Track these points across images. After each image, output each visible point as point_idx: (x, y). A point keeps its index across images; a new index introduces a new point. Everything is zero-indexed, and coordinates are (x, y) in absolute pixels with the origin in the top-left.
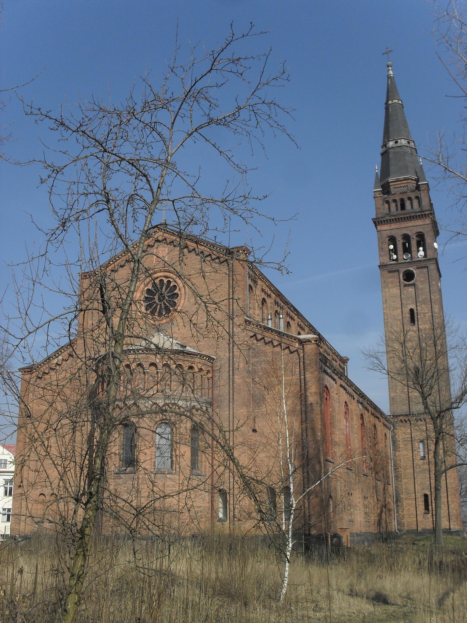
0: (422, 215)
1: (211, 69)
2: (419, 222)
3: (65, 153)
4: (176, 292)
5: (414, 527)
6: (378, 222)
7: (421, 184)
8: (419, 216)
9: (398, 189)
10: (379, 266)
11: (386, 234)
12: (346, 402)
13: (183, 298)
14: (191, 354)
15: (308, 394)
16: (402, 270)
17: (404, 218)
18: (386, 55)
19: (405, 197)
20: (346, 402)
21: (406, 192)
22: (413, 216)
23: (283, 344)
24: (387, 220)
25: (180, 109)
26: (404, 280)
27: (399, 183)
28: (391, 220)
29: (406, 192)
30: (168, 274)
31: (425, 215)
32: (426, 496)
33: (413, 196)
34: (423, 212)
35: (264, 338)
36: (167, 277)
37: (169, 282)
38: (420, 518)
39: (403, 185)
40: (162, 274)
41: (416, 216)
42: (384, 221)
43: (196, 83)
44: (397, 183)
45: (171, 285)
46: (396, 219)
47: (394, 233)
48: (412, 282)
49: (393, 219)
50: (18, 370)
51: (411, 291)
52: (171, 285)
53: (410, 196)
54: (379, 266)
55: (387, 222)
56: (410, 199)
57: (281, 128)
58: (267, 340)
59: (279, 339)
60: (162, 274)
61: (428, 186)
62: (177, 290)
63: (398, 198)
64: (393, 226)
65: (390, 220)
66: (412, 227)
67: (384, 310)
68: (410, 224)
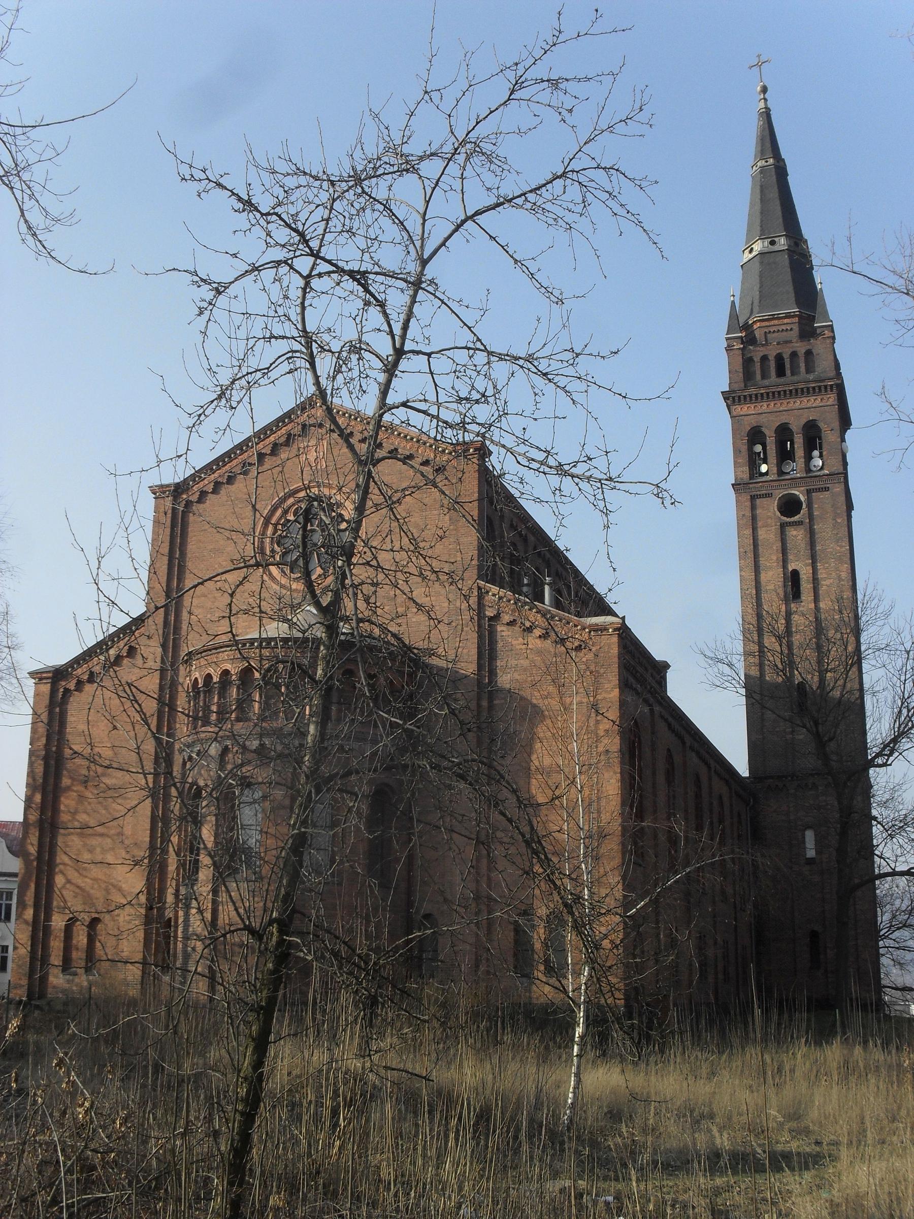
0: (820, 387)
1: (509, 99)
2: (814, 401)
3: (235, 255)
6: (733, 398)
7: (819, 327)
8: (814, 388)
9: (776, 334)
10: (733, 485)
11: (748, 424)
12: (669, 750)
16: (779, 494)
17: (785, 391)
18: (756, 69)
20: (669, 750)
21: (790, 342)
22: (802, 389)
24: (750, 396)
25: (443, 173)
26: (782, 513)
27: (776, 322)
28: (759, 396)
29: (790, 342)
31: (826, 387)
32: (814, 935)
34: (823, 381)
39: (784, 327)
41: (808, 388)
42: (745, 396)
43: (477, 123)
44: (772, 323)
46: (768, 394)
47: (763, 420)
48: (796, 518)
49: (762, 394)
50: (28, 676)
51: (796, 536)
53: (798, 349)
54: (733, 485)
55: (751, 400)
57: (632, 218)
61: (833, 331)
63: (772, 352)
64: (764, 407)
65: (756, 395)
66: (797, 411)
67: (741, 570)
68: (797, 403)
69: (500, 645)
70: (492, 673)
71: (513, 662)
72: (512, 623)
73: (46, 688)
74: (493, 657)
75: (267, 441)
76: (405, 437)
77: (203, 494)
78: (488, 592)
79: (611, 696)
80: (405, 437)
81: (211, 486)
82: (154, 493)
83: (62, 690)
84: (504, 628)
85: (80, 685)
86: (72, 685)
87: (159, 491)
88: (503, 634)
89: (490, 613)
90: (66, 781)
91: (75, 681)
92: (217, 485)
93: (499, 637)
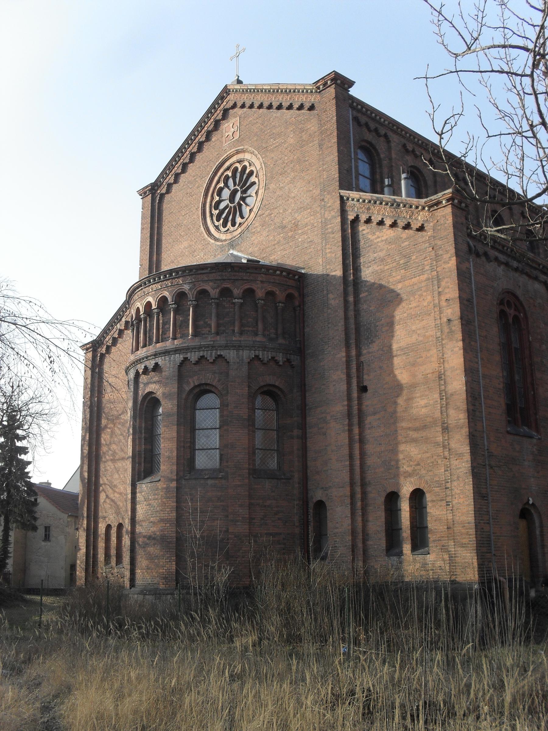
15: (443, 303)
30: (240, 156)
37: (244, 168)
69: (362, 243)
70: (357, 270)
71: (372, 256)
72: (368, 221)
73: (90, 355)
74: (356, 255)
75: (203, 132)
76: (286, 91)
77: (170, 186)
78: (348, 199)
79: (449, 265)
80: (286, 91)
81: (173, 178)
82: (141, 195)
83: (99, 355)
84: (364, 227)
85: (108, 349)
86: (104, 350)
87: (143, 193)
88: (364, 232)
89: (351, 217)
90: (104, 422)
91: (105, 347)
92: (177, 176)
93: (361, 236)
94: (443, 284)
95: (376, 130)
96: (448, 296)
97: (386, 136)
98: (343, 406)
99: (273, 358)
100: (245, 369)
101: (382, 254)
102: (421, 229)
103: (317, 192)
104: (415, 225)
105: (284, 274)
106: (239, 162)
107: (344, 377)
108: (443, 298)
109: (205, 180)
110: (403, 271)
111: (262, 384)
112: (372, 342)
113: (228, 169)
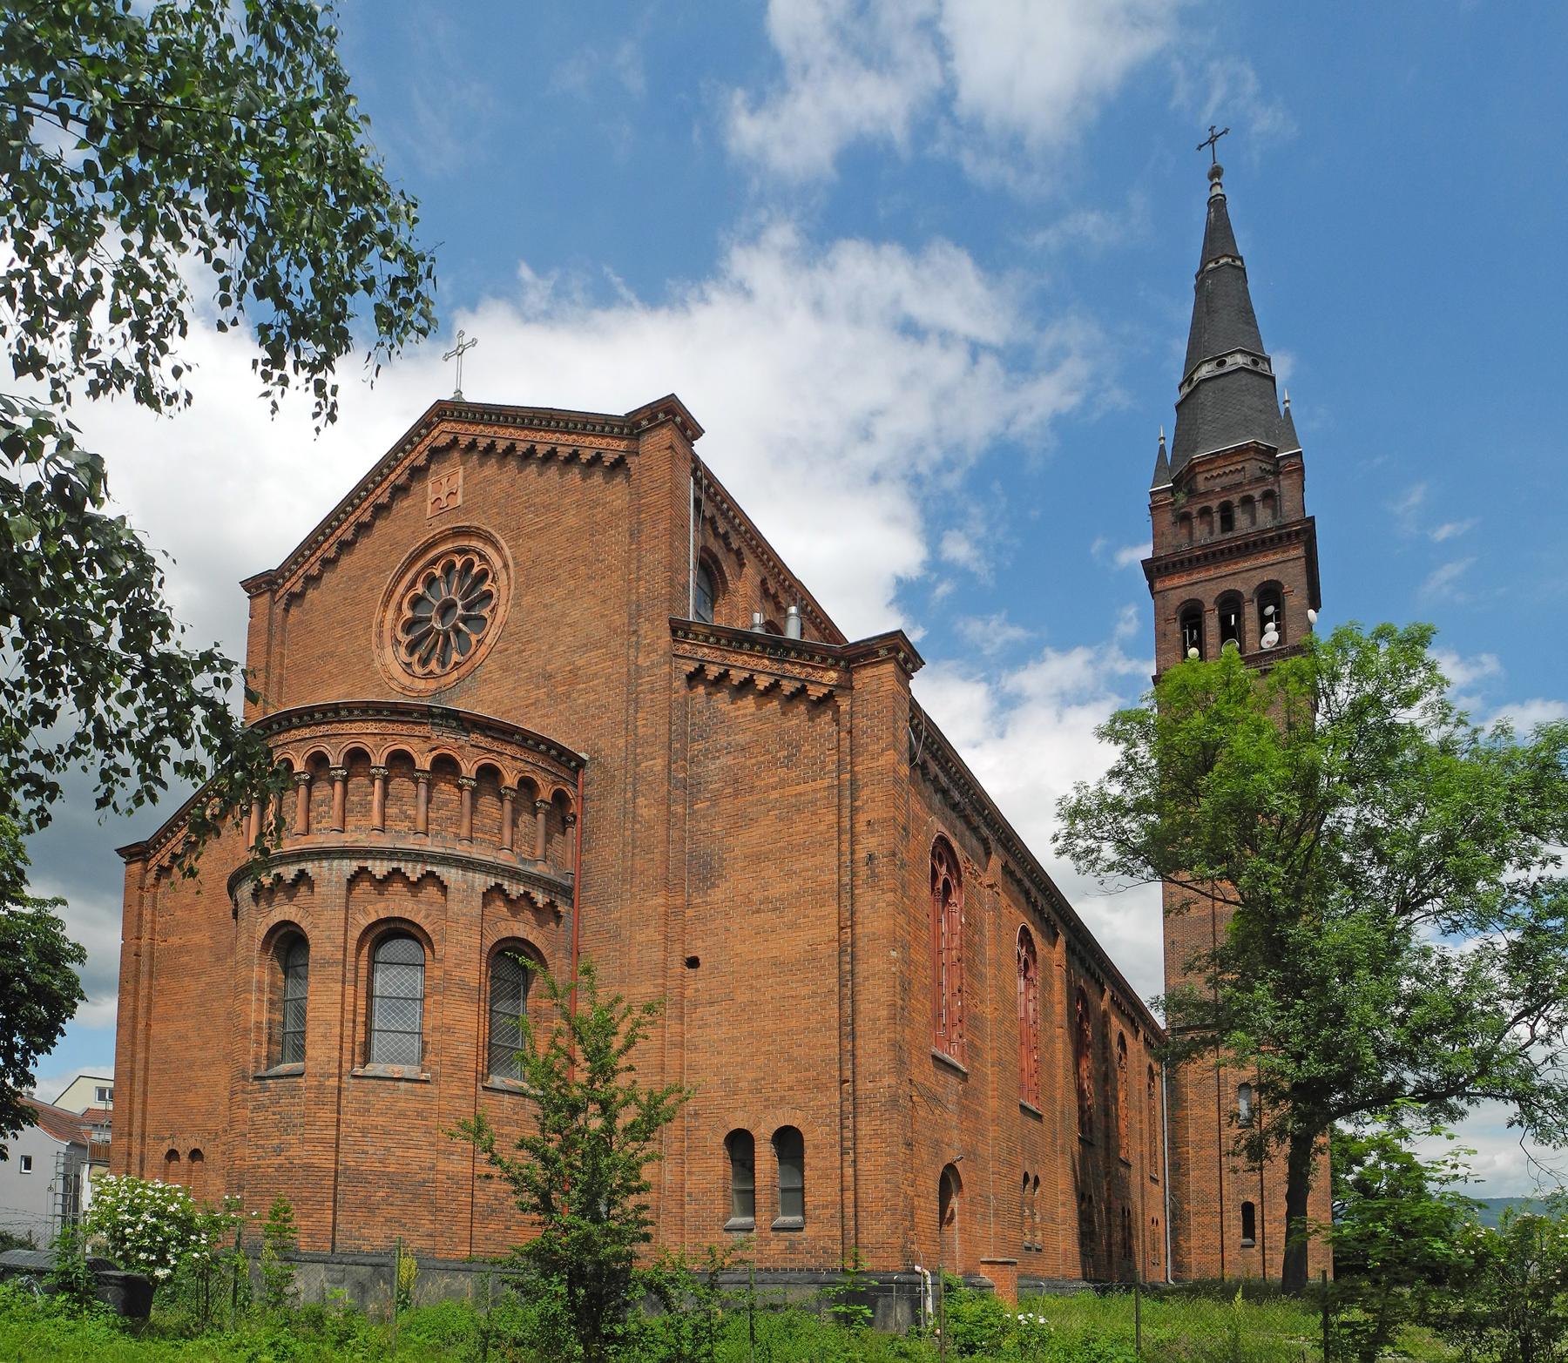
4: (485, 587)
5: (1215, 1272)
13: (503, 601)
14: (490, 729)
15: (861, 827)
19: (1235, 498)
23: (784, 682)
30: (464, 543)
33: (1257, 494)
35: (727, 671)
36: (461, 551)
37: (469, 565)
38: (1232, 1254)
40: (449, 546)
45: (475, 570)
52: (475, 570)
56: (1247, 501)
58: (737, 676)
59: (775, 667)
60: (449, 546)
62: (477, 563)
71: (723, 740)
94: (865, 794)
95: (725, 537)
96: (871, 816)
97: (738, 553)
98: (656, 986)
99: (526, 894)
100: (478, 901)
101: (741, 739)
102: (827, 700)
103: (619, 620)
104: (815, 692)
105: (553, 752)
106: (461, 551)
107: (658, 937)
108: (862, 818)
109: (386, 577)
110: (782, 772)
111: (506, 934)
112: (714, 885)
113: (434, 562)
